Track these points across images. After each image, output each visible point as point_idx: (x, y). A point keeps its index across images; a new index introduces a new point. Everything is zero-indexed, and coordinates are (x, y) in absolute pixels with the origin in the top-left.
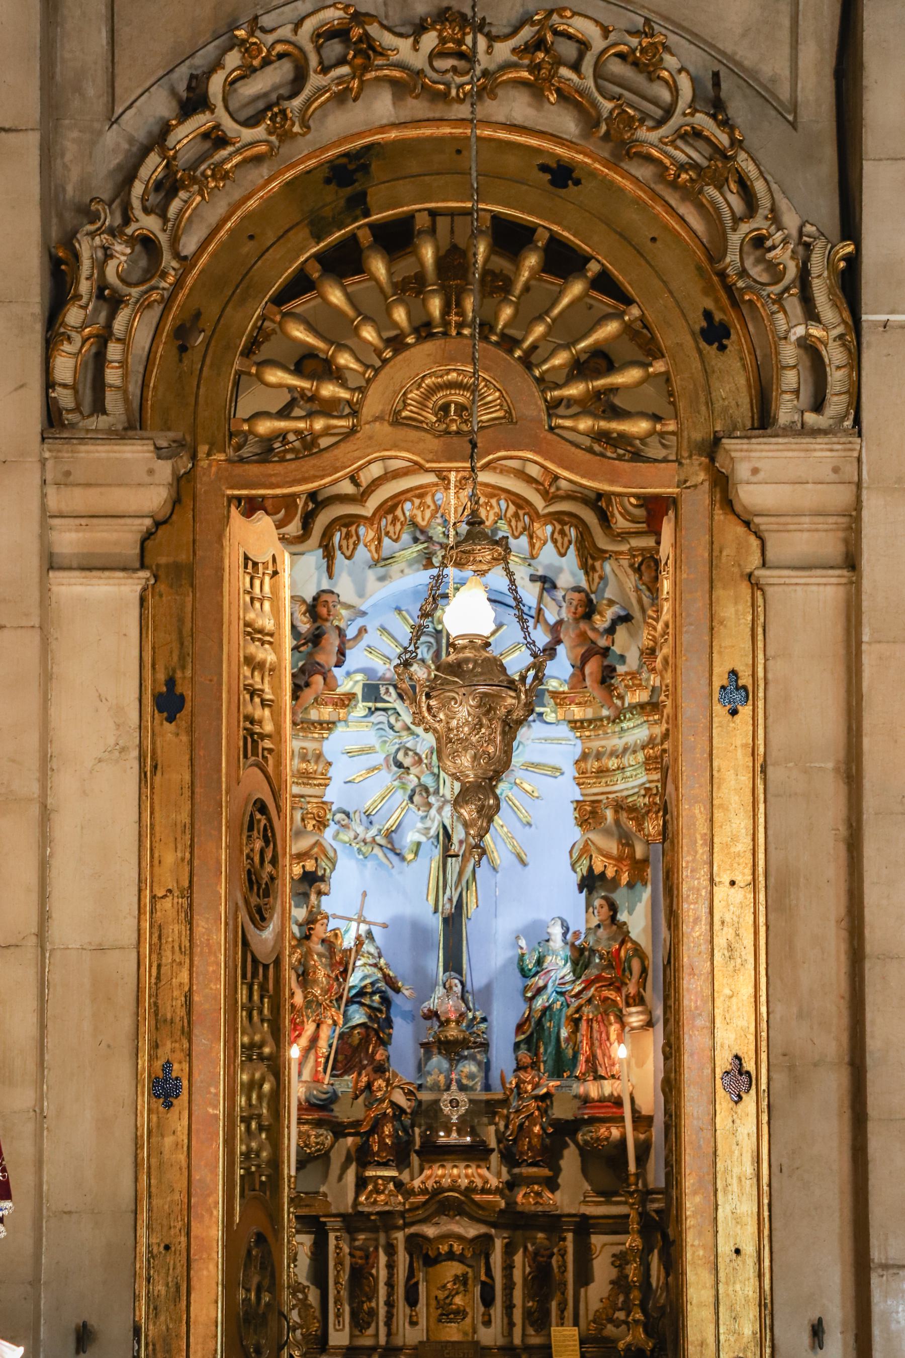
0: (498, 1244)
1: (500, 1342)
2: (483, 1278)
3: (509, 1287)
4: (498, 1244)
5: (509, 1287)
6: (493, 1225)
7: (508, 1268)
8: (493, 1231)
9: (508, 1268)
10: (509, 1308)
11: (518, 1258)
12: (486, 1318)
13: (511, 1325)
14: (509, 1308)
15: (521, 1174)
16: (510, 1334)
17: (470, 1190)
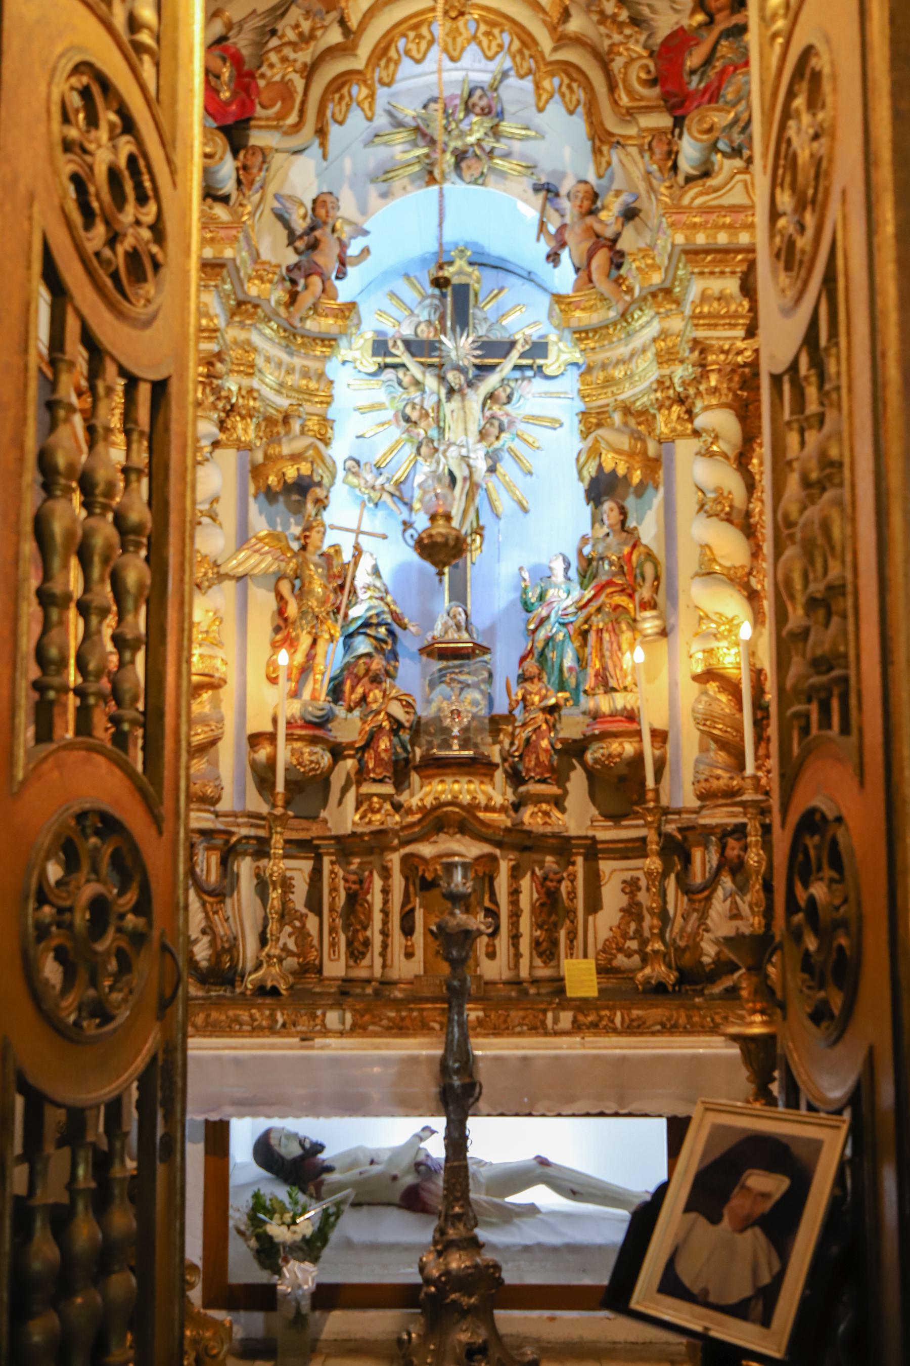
0: (504, 867)
1: (506, 975)
2: (487, 904)
3: (515, 915)
4: (504, 867)
5: (515, 915)
6: (499, 844)
7: (515, 893)
8: (498, 852)
9: (515, 893)
10: (515, 938)
11: (526, 883)
12: (490, 949)
13: (518, 955)
14: (515, 938)
15: (528, 792)
16: (517, 966)
17: (472, 808)
